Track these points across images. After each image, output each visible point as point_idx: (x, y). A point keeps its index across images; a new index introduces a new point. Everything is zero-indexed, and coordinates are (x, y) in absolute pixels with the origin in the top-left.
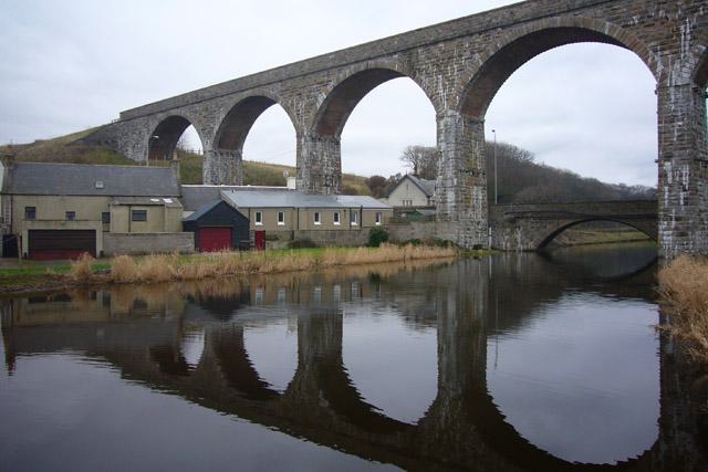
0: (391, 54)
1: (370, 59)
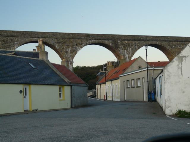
1: (100, 39)
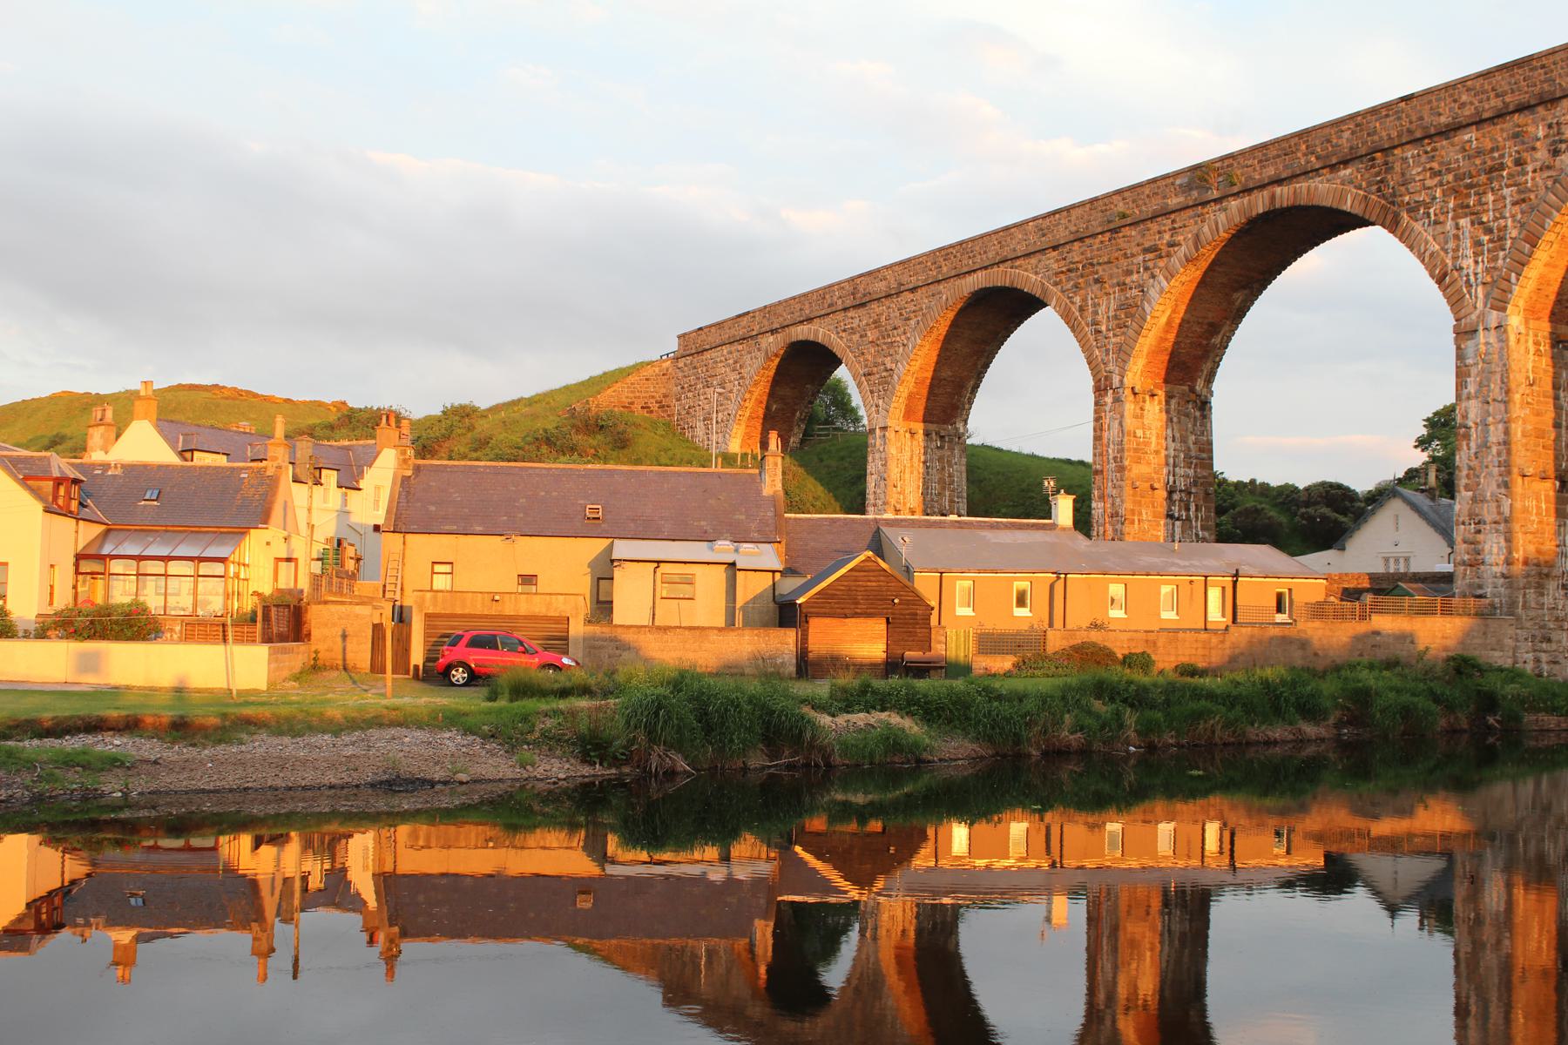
0: (1333, 168)
1: (1279, 182)
